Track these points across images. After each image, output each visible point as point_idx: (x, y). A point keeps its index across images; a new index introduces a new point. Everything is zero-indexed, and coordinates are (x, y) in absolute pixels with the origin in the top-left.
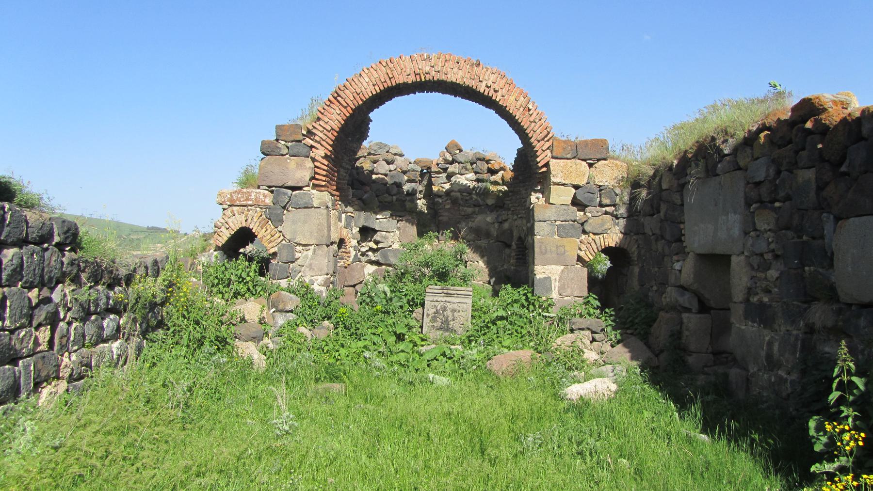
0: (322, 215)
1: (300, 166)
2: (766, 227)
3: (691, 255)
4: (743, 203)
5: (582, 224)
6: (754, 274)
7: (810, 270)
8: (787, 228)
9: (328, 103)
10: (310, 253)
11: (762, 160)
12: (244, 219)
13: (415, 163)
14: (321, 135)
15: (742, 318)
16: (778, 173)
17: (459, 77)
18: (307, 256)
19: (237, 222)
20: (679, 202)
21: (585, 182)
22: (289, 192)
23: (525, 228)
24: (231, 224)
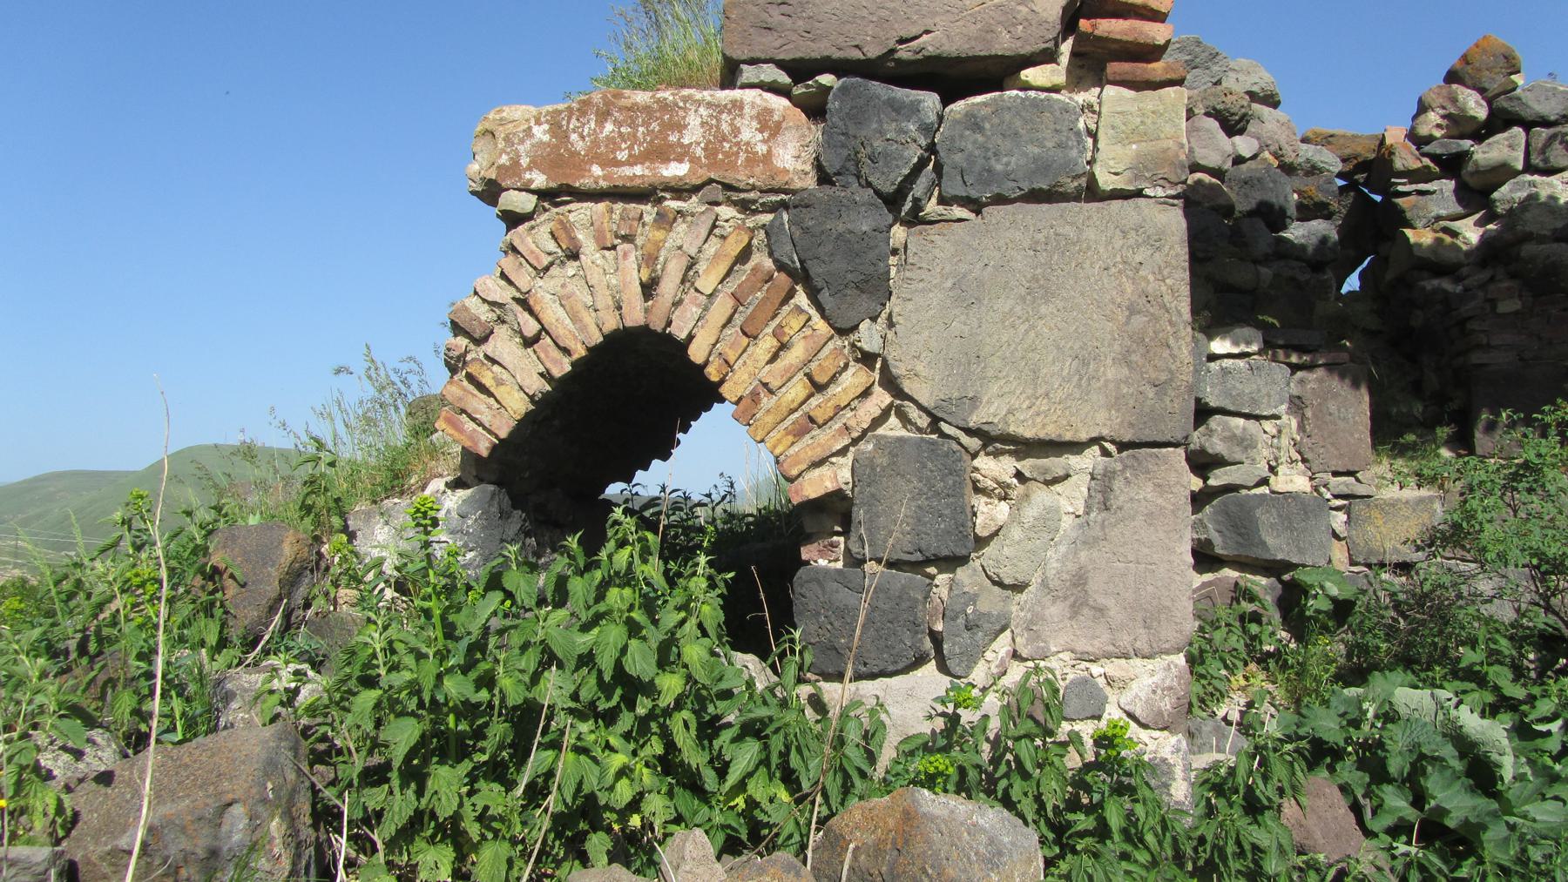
0: (1156, 242)
10: (1071, 498)
18: (1048, 522)
19: (589, 298)
24: (553, 314)
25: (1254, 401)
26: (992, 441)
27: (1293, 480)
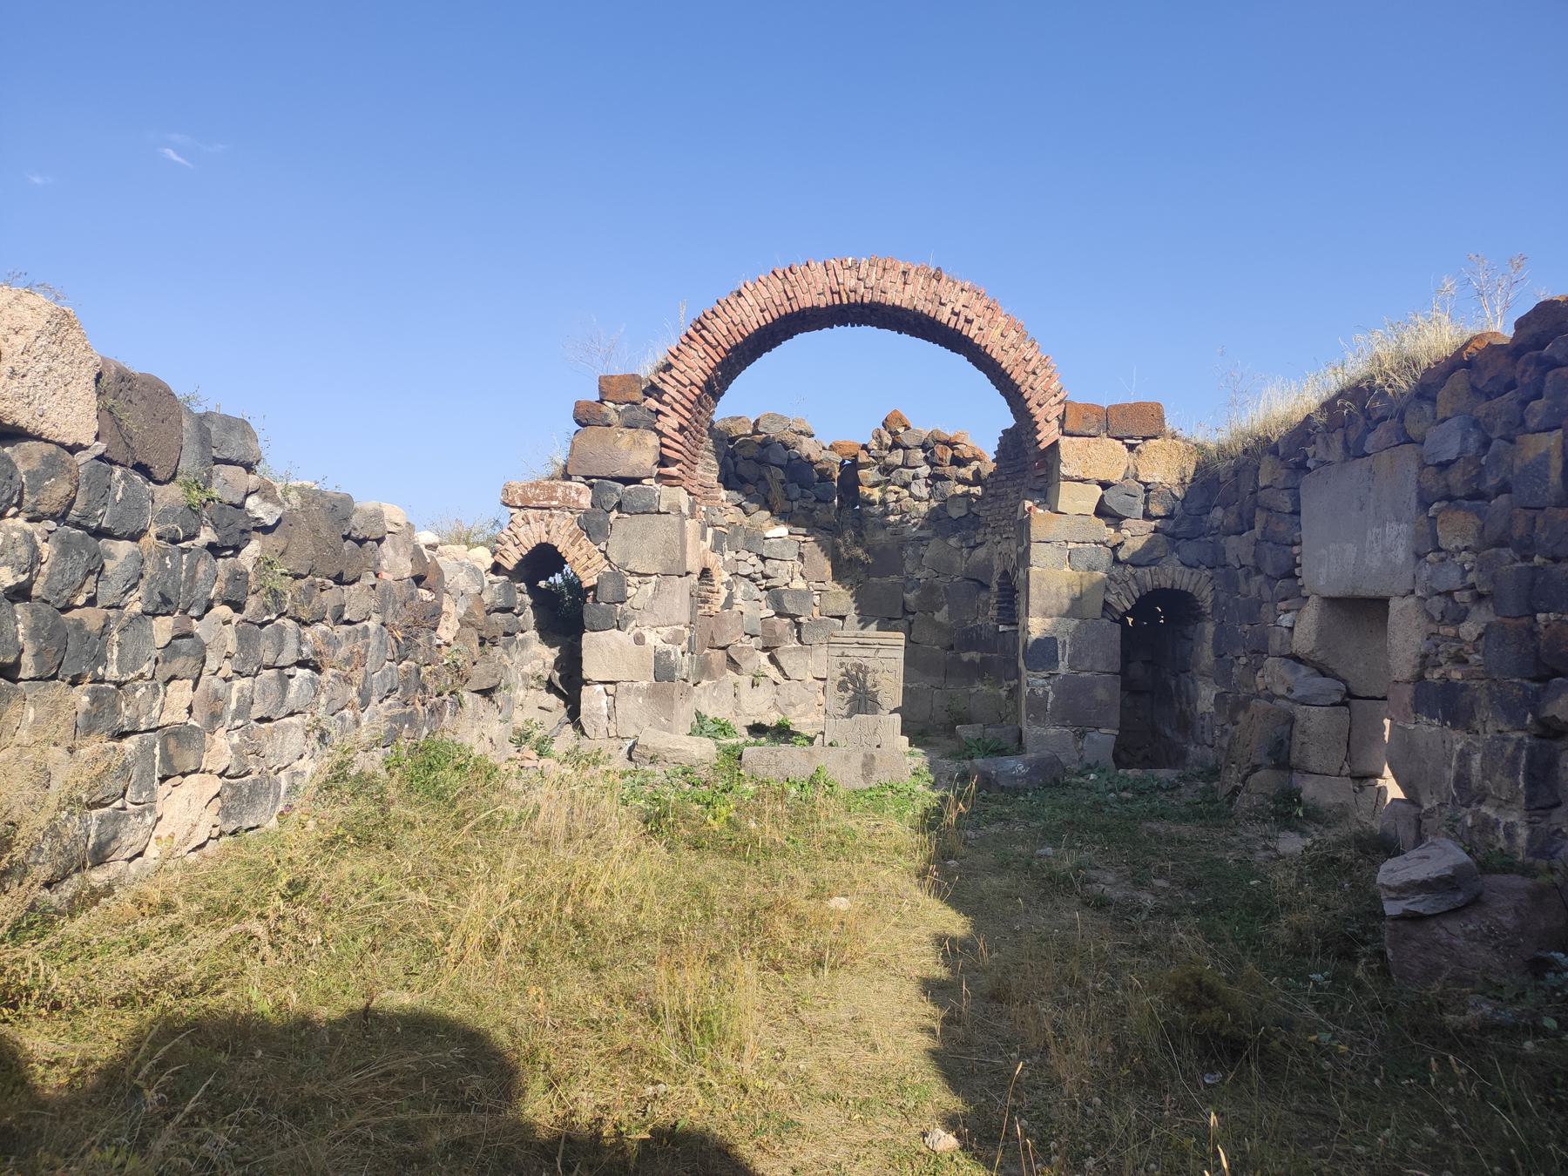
1: (636, 443)
2: (1459, 543)
3: (1313, 599)
4: (1414, 503)
5: (1114, 549)
6: (1433, 628)
7: (1547, 619)
8: (1501, 544)
9: (686, 340)
10: (650, 588)
11: (1454, 422)
12: (544, 529)
13: (832, 448)
14: (673, 392)
15: (1410, 710)
16: (1486, 444)
17: (907, 296)
18: (646, 592)
19: (531, 535)
20: (1288, 508)
21: (1120, 477)
22: (620, 486)
23: (1014, 556)
24: (523, 538)
26: (631, 573)
27: (799, 584)
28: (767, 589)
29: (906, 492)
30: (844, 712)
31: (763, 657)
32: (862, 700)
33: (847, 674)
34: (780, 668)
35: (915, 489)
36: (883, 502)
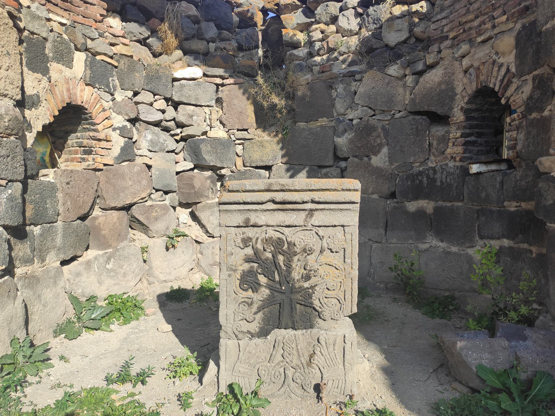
25: (197, 99)
27: (219, 133)
28: (183, 139)
29: (333, 28)
30: (254, 327)
31: (184, 214)
32: (288, 305)
33: (256, 257)
34: (202, 226)
35: (343, 22)
36: (310, 43)
